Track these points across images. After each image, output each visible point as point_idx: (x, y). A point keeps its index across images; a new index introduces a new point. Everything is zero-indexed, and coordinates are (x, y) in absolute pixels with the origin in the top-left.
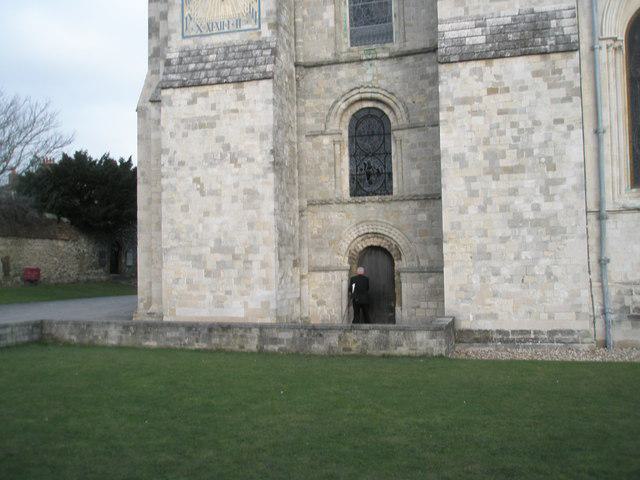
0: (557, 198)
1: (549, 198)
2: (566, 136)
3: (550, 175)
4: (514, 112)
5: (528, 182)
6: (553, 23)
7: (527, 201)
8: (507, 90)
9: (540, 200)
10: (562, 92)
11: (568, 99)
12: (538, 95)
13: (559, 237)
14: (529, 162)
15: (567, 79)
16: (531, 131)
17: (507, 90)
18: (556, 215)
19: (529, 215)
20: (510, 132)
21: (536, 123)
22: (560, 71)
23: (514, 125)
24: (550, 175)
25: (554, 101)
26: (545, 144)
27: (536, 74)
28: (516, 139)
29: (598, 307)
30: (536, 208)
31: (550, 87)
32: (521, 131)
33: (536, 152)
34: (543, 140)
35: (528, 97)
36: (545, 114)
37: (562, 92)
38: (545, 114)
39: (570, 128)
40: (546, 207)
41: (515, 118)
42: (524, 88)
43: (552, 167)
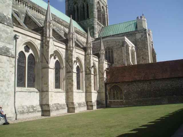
0: (9, 88)
1: (8, 88)
3: (9, 83)
4: (3, 68)
5: (5, 84)
7: (4, 88)
8: (2, 63)
9: (6, 88)
12: (8, 65)
14: (5, 80)
16: (6, 73)
17: (2, 63)
19: (5, 91)
20: (2, 72)
21: (7, 71)
23: (3, 71)
24: (9, 83)
26: (8, 76)
27: (8, 61)
28: (3, 74)
30: (6, 90)
32: (4, 72)
33: (6, 77)
36: (9, 70)
38: (9, 70)
40: (8, 90)
41: (3, 69)
42: (5, 63)
43: (9, 81)
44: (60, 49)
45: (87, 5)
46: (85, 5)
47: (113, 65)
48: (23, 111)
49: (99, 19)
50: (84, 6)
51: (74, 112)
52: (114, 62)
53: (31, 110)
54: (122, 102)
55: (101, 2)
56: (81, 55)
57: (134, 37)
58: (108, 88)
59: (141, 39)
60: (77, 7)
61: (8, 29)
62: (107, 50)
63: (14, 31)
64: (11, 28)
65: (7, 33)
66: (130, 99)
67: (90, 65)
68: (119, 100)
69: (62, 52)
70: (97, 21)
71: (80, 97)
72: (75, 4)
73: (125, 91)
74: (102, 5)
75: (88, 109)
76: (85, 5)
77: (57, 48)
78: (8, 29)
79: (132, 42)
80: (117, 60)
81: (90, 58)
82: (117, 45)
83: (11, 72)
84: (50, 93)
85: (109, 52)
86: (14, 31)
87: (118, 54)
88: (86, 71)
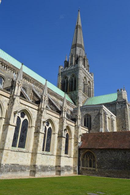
44: (30, 109)
45: (75, 79)
46: (73, 79)
47: (91, 132)
49: (84, 91)
50: (72, 80)
51: (34, 176)
52: (92, 128)
54: (94, 170)
55: (87, 78)
56: (55, 118)
57: (114, 108)
58: (82, 154)
59: (120, 110)
60: (67, 81)
66: (102, 169)
67: (63, 128)
68: (92, 168)
69: (33, 111)
70: (83, 93)
71: (48, 159)
72: (65, 78)
74: (88, 80)
75: (56, 174)
76: (73, 79)
77: (27, 107)
79: (112, 112)
80: (94, 127)
81: (63, 121)
82: (95, 113)
84: (5, 152)
85: (88, 119)
87: (96, 121)
88: (58, 134)
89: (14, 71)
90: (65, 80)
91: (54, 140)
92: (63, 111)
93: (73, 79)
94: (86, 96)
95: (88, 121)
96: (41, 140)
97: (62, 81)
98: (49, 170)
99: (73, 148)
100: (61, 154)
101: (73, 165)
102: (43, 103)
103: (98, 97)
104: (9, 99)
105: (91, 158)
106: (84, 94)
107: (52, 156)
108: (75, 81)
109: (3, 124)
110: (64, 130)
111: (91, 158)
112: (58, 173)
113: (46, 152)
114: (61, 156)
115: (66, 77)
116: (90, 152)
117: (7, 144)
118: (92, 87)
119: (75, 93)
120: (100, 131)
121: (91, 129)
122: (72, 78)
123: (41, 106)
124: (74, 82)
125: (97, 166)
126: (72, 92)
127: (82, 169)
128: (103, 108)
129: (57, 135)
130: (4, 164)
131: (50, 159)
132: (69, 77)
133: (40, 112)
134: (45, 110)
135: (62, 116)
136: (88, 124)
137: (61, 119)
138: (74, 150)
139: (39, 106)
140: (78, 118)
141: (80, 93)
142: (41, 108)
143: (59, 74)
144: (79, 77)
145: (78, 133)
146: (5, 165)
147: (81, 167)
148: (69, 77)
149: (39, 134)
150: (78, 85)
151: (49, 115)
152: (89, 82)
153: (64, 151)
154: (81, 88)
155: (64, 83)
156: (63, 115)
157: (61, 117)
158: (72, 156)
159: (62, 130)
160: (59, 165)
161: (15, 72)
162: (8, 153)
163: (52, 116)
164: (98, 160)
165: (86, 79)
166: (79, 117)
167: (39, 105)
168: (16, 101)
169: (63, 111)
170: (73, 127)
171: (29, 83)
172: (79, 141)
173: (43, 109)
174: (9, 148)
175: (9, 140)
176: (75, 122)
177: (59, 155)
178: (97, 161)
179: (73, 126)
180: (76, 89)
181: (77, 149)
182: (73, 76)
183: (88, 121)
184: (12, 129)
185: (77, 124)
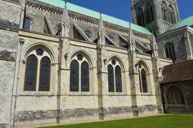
1: (4, 92)
2: (10, 79)
3: (5, 87)
6: (11, 55)
10: (10, 69)
11: (12, 71)
12: (5, 69)
13: (5, 101)
15: (12, 67)
18: (5, 96)
21: (3, 75)
22: (11, 65)
24: (5, 87)
25: (8, 71)
27: (5, 64)
29: (12, 118)
31: (8, 68)
34: (4, 79)
35: (2, 69)
36: (6, 73)
37: (10, 69)
38: (6, 73)
39: (11, 77)
43: (6, 86)
44: (87, 50)
45: (151, 7)
47: (176, 62)
48: (25, 117)
49: (165, 18)
51: (103, 119)
53: (38, 116)
54: (184, 108)
56: (121, 54)
61: (10, 34)
62: (167, 46)
63: (19, 35)
64: (15, 33)
65: (9, 38)
69: (90, 52)
70: (163, 21)
72: (139, 11)
73: (187, 93)
74: (168, 3)
75: (134, 115)
76: (149, 8)
78: (10, 34)
80: (179, 55)
81: (132, 56)
83: (8, 75)
85: (170, 48)
86: (19, 35)
88: (129, 71)
89: (73, 16)
90: (140, 12)
91: (125, 78)
92: (130, 44)
93: (149, 9)
94: (169, 23)
95: (170, 52)
96: (105, 80)
97: (136, 15)
98: (124, 112)
99: (154, 85)
100: (135, 93)
101: (157, 104)
102: (100, 40)
103: (185, 20)
104: (58, 44)
105: (178, 93)
106: (165, 21)
107: (125, 96)
108: (152, 10)
109: (58, 70)
110: (134, 65)
111: (178, 93)
112: (136, 114)
113: (117, 93)
114: (135, 95)
115: (140, 9)
116: (175, 86)
117: (63, 89)
118: (175, 11)
119: (153, 24)
120: (188, 59)
121: (176, 60)
122: (147, 7)
123: (99, 44)
124: (150, 11)
125: (186, 102)
126: (150, 23)
127: (168, 107)
128: (188, 30)
129: (127, 73)
130: (63, 110)
131: (123, 100)
132: (144, 8)
133: (99, 51)
134: (104, 47)
135: (130, 50)
136: (171, 54)
137: (129, 54)
138: (155, 86)
139: (97, 45)
140: (154, 49)
141: (159, 21)
142: (99, 46)
143: (132, 8)
144: (155, 4)
145: (156, 67)
146: (64, 110)
147: (166, 105)
148: (144, 8)
149: (101, 74)
150: (155, 13)
151: (112, 52)
152: (170, 6)
153: (138, 89)
154: (160, 15)
155: (140, 16)
156: (131, 48)
157: (129, 51)
158: (154, 94)
159: (133, 66)
160: (135, 105)
161: (75, 17)
162: (65, 98)
163: (117, 53)
164: (187, 94)
165: (165, 4)
166: (154, 47)
167: (97, 43)
168: (64, 44)
169: (130, 44)
170: (149, 61)
171: (93, 25)
172: (160, 75)
173: (101, 46)
174: (66, 93)
175: (64, 85)
176: (151, 54)
177: (133, 94)
178: (185, 96)
179: (148, 60)
180: (154, 19)
181: (158, 85)
182: (148, 5)
183: (170, 52)
184: (66, 73)
185: (154, 56)
